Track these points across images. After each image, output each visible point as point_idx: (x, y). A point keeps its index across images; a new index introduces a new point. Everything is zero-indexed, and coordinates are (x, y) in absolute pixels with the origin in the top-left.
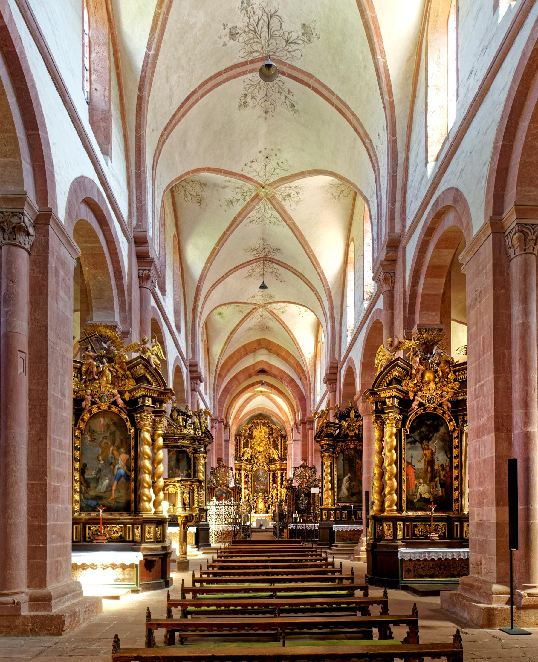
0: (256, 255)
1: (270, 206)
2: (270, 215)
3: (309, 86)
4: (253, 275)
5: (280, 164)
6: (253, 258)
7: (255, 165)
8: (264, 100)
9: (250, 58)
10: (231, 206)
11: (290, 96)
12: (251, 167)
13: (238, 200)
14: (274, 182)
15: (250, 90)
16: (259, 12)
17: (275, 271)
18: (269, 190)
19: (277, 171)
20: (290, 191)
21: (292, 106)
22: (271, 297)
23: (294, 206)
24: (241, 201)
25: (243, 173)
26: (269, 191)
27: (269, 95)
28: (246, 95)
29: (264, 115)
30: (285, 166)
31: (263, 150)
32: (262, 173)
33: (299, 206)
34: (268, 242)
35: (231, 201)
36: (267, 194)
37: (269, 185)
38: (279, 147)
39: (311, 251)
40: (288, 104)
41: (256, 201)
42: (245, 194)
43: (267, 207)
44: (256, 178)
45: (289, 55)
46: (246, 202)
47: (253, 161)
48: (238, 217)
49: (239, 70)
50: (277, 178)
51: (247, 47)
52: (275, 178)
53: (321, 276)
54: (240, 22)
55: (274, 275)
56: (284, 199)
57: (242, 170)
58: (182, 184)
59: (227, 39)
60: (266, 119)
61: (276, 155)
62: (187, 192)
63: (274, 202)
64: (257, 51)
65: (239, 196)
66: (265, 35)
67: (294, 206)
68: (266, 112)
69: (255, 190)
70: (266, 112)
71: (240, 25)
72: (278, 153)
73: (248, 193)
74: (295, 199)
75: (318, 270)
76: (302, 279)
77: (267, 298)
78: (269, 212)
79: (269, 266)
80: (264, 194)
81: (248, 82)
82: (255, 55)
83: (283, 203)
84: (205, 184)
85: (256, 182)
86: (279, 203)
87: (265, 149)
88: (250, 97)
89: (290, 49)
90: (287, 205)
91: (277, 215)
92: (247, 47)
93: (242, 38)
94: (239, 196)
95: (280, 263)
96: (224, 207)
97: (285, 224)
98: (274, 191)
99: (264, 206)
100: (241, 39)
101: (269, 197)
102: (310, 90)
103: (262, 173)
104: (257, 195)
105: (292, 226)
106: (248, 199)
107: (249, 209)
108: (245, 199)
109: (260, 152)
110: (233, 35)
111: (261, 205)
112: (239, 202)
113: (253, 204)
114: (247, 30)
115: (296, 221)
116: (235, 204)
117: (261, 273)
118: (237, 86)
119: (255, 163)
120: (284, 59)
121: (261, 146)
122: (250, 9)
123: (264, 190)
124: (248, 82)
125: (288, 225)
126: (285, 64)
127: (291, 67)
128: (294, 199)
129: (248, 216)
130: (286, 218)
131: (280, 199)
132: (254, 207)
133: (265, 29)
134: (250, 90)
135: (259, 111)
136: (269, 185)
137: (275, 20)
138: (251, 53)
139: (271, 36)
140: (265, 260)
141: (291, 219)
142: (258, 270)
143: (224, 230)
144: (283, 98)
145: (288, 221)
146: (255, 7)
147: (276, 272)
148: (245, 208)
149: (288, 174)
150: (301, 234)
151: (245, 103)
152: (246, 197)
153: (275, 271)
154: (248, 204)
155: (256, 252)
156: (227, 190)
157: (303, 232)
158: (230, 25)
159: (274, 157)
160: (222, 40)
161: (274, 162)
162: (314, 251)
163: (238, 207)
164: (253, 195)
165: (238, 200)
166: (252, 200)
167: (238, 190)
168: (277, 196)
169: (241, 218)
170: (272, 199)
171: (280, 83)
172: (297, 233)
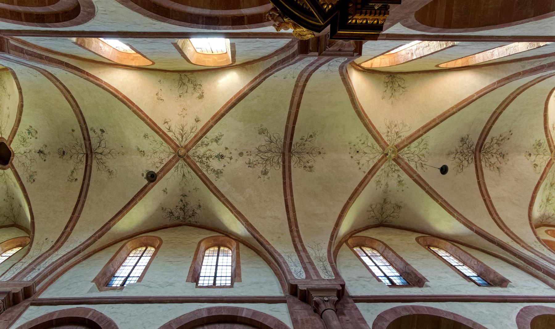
0: (470, 162)
1: (406, 149)
2: (416, 149)
3: (294, 127)
4: (498, 165)
5: (362, 142)
6: (473, 165)
7: (362, 162)
8: (311, 155)
9: (282, 163)
10: (403, 182)
11: (305, 138)
12: (363, 165)
13: (399, 176)
14: (381, 146)
15: (302, 164)
16: (258, 157)
17: (495, 141)
18: (389, 151)
19: (369, 144)
20: (393, 132)
21: (311, 136)
22: (539, 145)
23: (407, 128)
24: (399, 173)
25: (367, 172)
26: (390, 150)
27: (307, 151)
28: (305, 167)
29: (322, 154)
30: (364, 139)
31: (351, 155)
32: (371, 156)
33: (407, 124)
34: (453, 150)
35: (399, 182)
36: (393, 152)
37: (384, 150)
38: (347, 143)
39: (453, 108)
40: (310, 139)
41: (399, 161)
42: (394, 170)
43: (408, 152)
44: (376, 161)
45: (279, 140)
46: (400, 169)
47: (359, 163)
48: (413, 177)
49: (287, 170)
50: (376, 144)
51: (274, 165)
52: (376, 145)
53: (481, 95)
54: (260, 168)
55: (502, 143)
56: (400, 137)
57: (364, 172)
58: (385, 217)
59: (266, 177)
60: (325, 153)
61: (354, 145)
62: (391, 215)
63: (401, 146)
64: (278, 159)
65: (395, 175)
66: (269, 155)
67: (407, 128)
68: (320, 153)
69: (389, 161)
70: (320, 153)
71: (261, 169)
72: (353, 144)
73: (393, 167)
74: (401, 128)
75: (474, 98)
76: (501, 113)
77: (542, 149)
78: (412, 150)
79: (489, 147)
80: (394, 155)
81: (296, 165)
82: (280, 160)
83: (403, 138)
84: (385, 200)
85: (379, 161)
86: (403, 142)
87: (350, 153)
88: (307, 164)
89: (275, 140)
90: (405, 134)
91: (416, 143)
92: (274, 165)
93: (268, 168)
94: (395, 175)
95: (483, 136)
96: (404, 188)
97: (424, 136)
98: (391, 145)
99: (405, 155)
100: (269, 168)
101: (396, 150)
102: (296, 126)
103: (371, 156)
104: (394, 160)
105: (425, 129)
106: (398, 168)
107: (406, 168)
108: (398, 170)
109: (352, 157)
110: (265, 173)
111: (405, 157)
112: (401, 175)
113: (402, 163)
114: (265, 165)
115: (422, 126)
116: (402, 179)
117: (498, 156)
118: (297, 171)
119: (360, 161)
120: (282, 143)
121: (346, 157)
122: (254, 163)
123: (389, 154)
124: (296, 165)
125: (425, 132)
126: (285, 143)
127: (285, 137)
128: (400, 129)
129: (415, 169)
130: (417, 135)
131: (399, 140)
132: (406, 163)
133: (266, 154)
134: (302, 164)
135: (318, 158)
136: (384, 150)
137: (261, 149)
138: (278, 163)
139: (270, 151)
140: (480, 151)
141: (419, 131)
142: (493, 160)
143: (423, 192)
144: (307, 142)
145: (421, 133)
146: (254, 160)
147: (498, 140)
148: (405, 170)
149: (370, 135)
150: (434, 120)
151: (310, 167)
152: (396, 169)
153: (495, 141)
154: (402, 168)
155: (465, 163)
156: (389, 184)
157: (432, 118)
158: (260, 174)
159: (357, 147)
160: (266, 179)
161: (362, 147)
162: (453, 105)
163: (405, 177)
164: (394, 163)
165: (399, 176)
166: (399, 164)
167: (390, 175)
168: (396, 143)
169: (414, 175)
170: (399, 148)
171: (298, 145)
172: (434, 124)
